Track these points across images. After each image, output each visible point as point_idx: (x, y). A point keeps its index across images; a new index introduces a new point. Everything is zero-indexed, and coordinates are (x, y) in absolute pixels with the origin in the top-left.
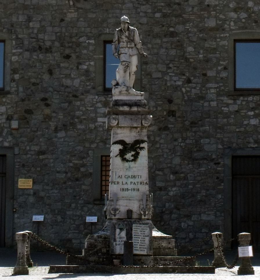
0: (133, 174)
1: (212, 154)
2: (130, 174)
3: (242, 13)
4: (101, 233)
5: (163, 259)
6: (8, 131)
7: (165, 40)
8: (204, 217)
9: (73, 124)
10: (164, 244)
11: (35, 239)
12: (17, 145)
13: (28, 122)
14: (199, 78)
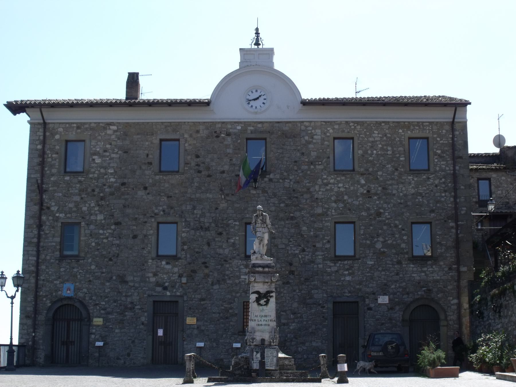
0: (265, 314)
1: (319, 301)
2: (263, 314)
3: (340, 204)
4: (243, 355)
5: (286, 373)
6: (179, 285)
7: (287, 222)
8: (314, 344)
9: (224, 280)
10: (287, 362)
11: (198, 359)
12: (186, 294)
13: (193, 278)
14: (310, 248)
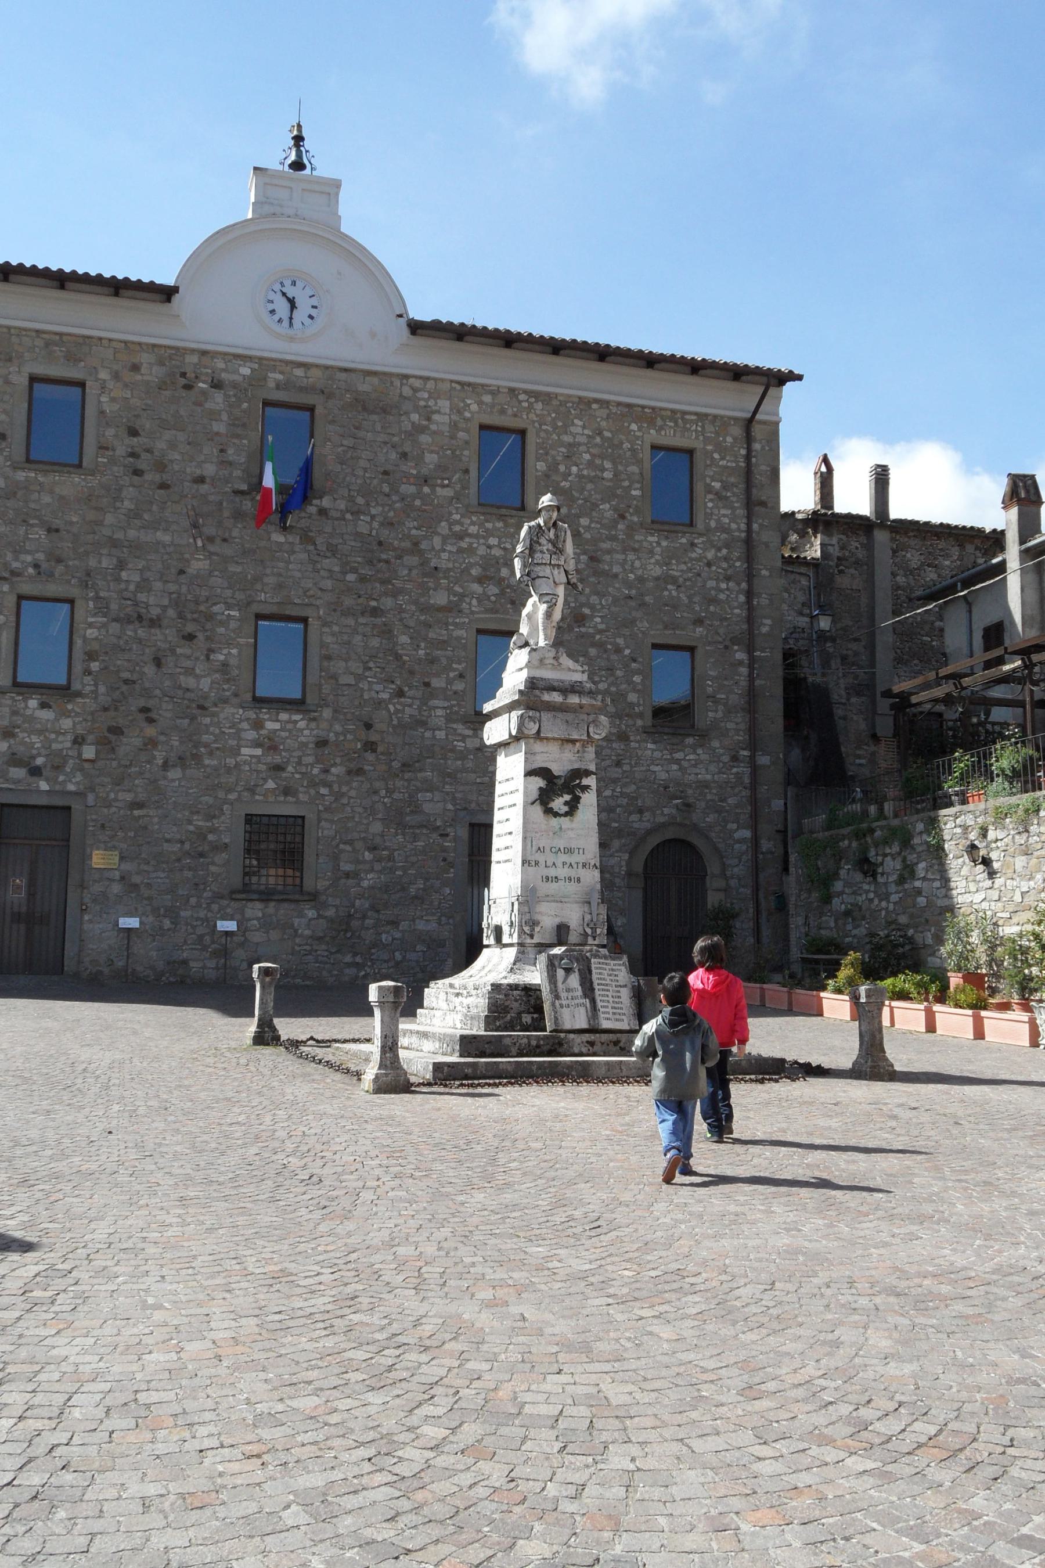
3: (491, 587)
7: (362, 620)
8: (421, 926)
9: (197, 757)
12: (92, 789)
13: (113, 749)
